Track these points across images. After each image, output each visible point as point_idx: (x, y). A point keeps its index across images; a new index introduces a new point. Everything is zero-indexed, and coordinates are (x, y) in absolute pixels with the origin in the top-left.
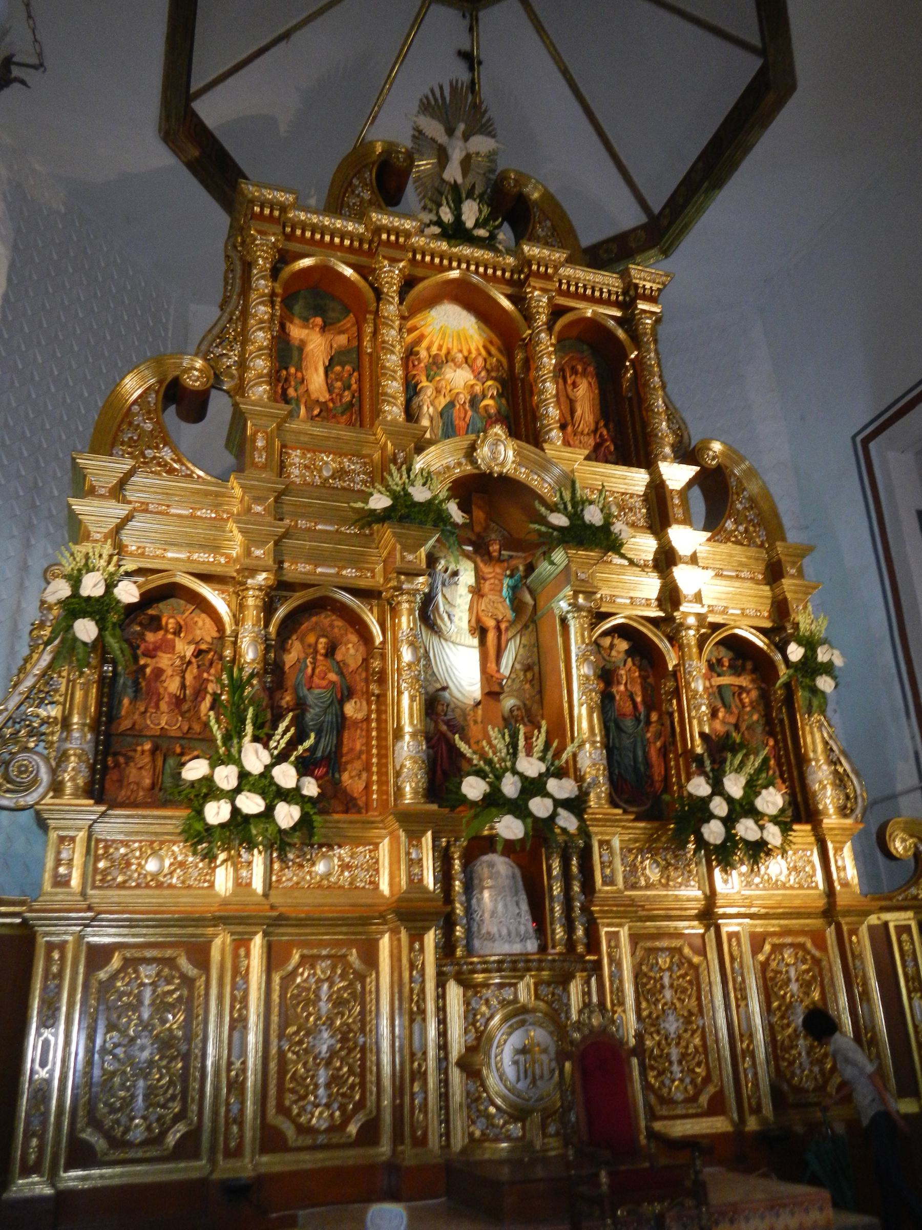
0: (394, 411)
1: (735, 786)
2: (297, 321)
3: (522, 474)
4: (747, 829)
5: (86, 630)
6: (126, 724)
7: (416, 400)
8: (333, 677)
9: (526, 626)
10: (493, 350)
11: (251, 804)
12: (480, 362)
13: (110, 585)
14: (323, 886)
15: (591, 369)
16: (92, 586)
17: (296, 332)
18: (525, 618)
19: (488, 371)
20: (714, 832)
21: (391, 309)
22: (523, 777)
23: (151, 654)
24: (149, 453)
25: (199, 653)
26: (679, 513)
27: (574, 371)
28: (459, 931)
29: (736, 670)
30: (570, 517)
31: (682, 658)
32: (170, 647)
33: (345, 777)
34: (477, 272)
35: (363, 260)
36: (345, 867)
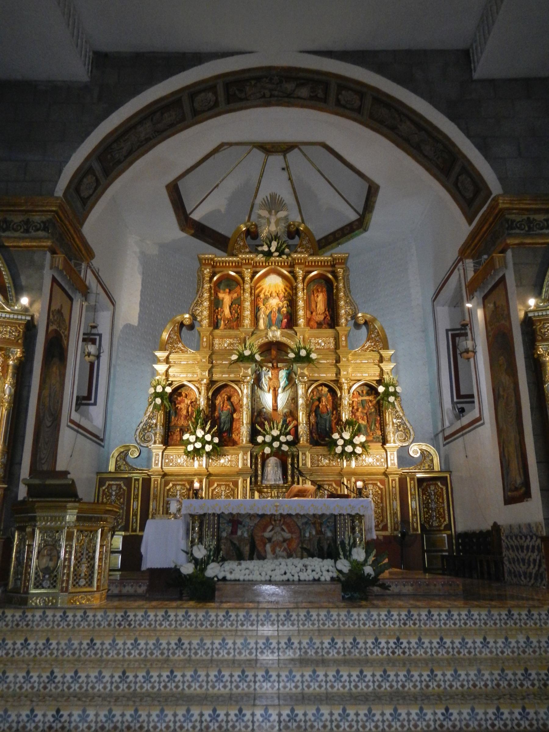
0: (247, 322)
1: (347, 436)
2: (221, 291)
3: (284, 340)
4: (349, 449)
5: (158, 401)
6: (173, 424)
7: (258, 314)
8: (229, 407)
9: (293, 385)
10: (287, 289)
11: (198, 445)
12: (282, 295)
13: (164, 388)
14: (223, 466)
15: (324, 289)
16: (159, 389)
17: (221, 295)
18: (293, 383)
19: (284, 297)
20: (339, 450)
21: (247, 286)
22: (273, 436)
23: (180, 403)
24: (176, 346)
25: (192, 402)
26: (344, 343)
27: (318, 291)
28: (259, 478)
29: (368, 394)
30: (295, 353)
31: (341, 393)
32: (184, 402)
33: (233, 435)
34: (278, 265)
35: (239, 270)
36: (229, 461)
